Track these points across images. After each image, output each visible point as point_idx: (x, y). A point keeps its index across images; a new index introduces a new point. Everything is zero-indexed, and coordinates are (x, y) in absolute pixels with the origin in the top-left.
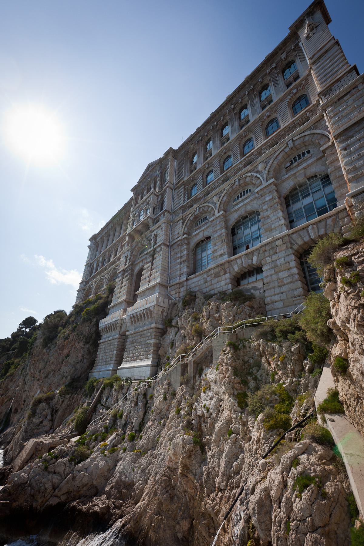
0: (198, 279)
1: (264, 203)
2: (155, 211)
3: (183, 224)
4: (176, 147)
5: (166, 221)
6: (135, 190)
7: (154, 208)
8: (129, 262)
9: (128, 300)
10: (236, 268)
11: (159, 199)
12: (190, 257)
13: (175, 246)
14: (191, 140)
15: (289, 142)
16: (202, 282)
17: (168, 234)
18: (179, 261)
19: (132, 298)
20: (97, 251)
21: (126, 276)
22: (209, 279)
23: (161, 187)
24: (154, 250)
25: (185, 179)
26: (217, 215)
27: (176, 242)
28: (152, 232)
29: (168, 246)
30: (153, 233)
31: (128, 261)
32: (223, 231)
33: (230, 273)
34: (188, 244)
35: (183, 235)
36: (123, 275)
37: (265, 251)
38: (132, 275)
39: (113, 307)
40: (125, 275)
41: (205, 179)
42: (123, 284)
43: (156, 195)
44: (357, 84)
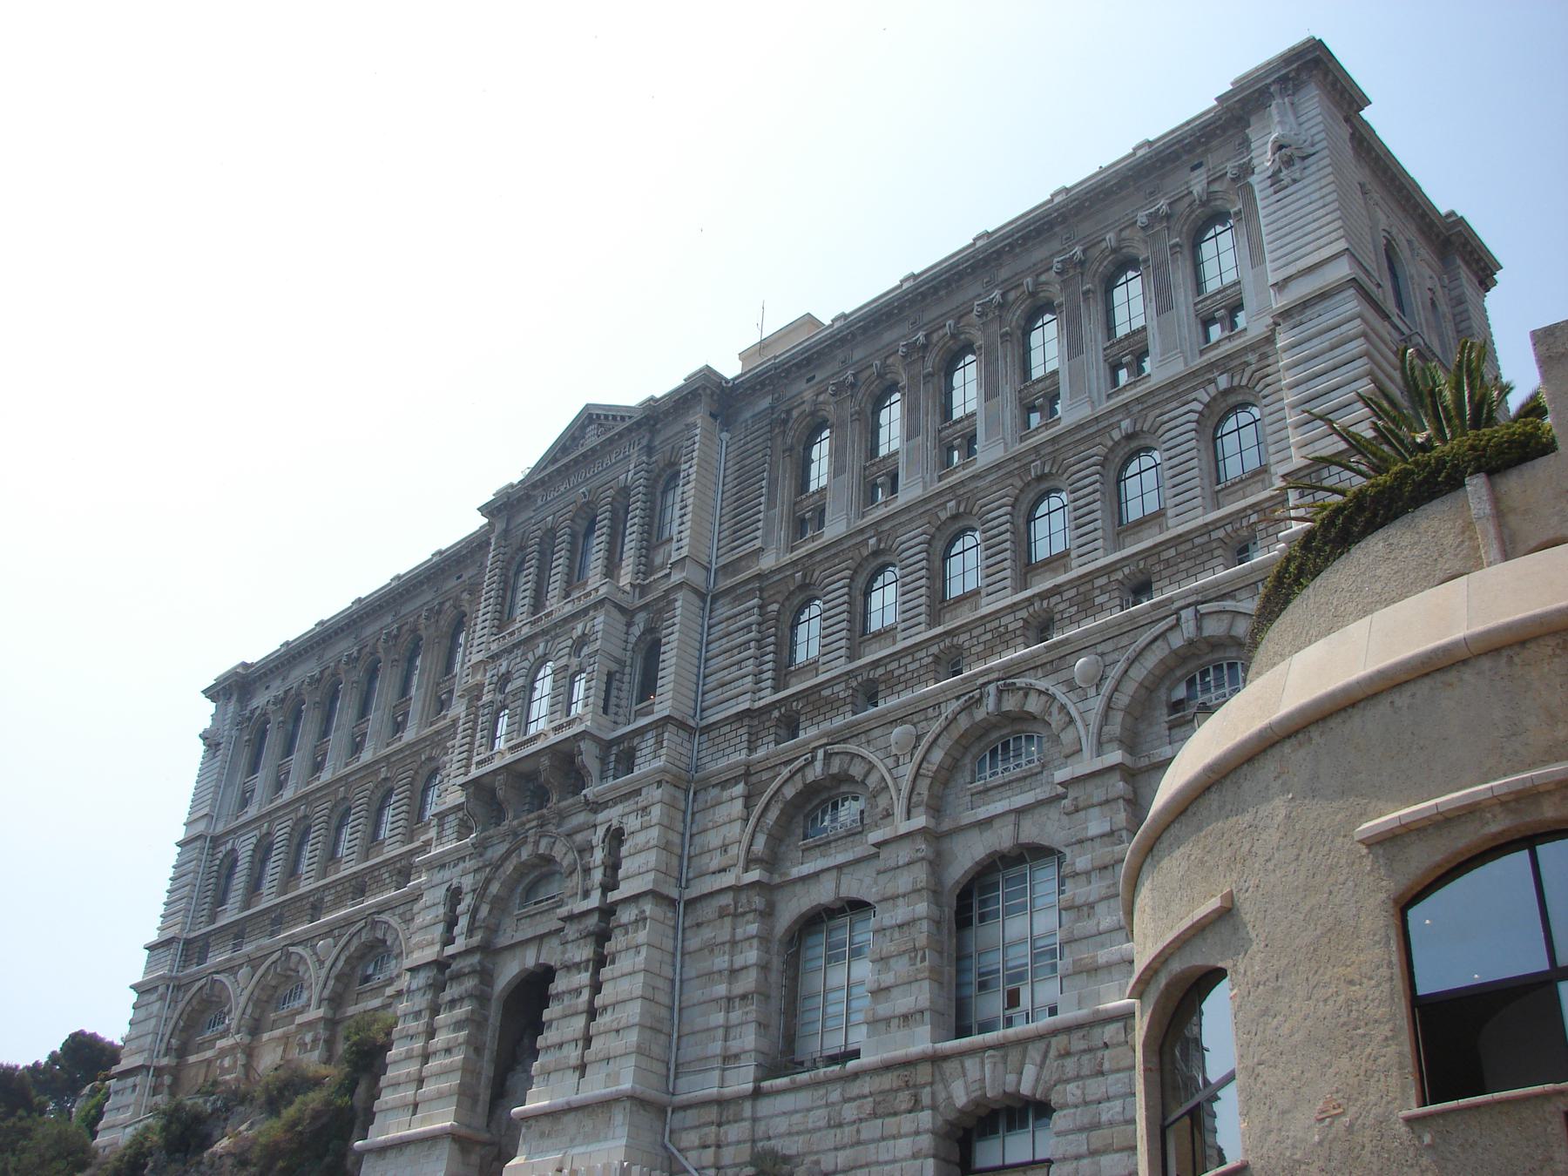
0: (803, 1099)
1: (1080, 842)
2: (614, 692)
3: (748, 806)
5: (668, 777)
6: (503, 507)
7: (610, 675)
8: (470, 932)
9: (464, 1131)
10: (961, 1097)
11: (637, 631)
12: (774, 977)
13: (709, 910)
14: (809, 360)
15: (1183, 613)
16: (818, 1117)
17: (676, 839)
18: (721, 989)
19: (480, 1119)
20: (254, 768)
21: (453, 1003)
22: (850, 1112)
23: (646, 566)
24: (607, 911)
25: (767, 562)
26: (904, 827)
27: (711, 894)
28: (595, 807)
29: (672, 903)
30: (601, 817)
31: (463, 922)
32: (922, 908)
33: (934, 1108)
34: (768, 913)
35: (746, 870)
37: (1068, 1054)
38: (481, 998)
39: (383, 1150)
40: (447, 995)
42: (441, 1039)
43: (622, 610)
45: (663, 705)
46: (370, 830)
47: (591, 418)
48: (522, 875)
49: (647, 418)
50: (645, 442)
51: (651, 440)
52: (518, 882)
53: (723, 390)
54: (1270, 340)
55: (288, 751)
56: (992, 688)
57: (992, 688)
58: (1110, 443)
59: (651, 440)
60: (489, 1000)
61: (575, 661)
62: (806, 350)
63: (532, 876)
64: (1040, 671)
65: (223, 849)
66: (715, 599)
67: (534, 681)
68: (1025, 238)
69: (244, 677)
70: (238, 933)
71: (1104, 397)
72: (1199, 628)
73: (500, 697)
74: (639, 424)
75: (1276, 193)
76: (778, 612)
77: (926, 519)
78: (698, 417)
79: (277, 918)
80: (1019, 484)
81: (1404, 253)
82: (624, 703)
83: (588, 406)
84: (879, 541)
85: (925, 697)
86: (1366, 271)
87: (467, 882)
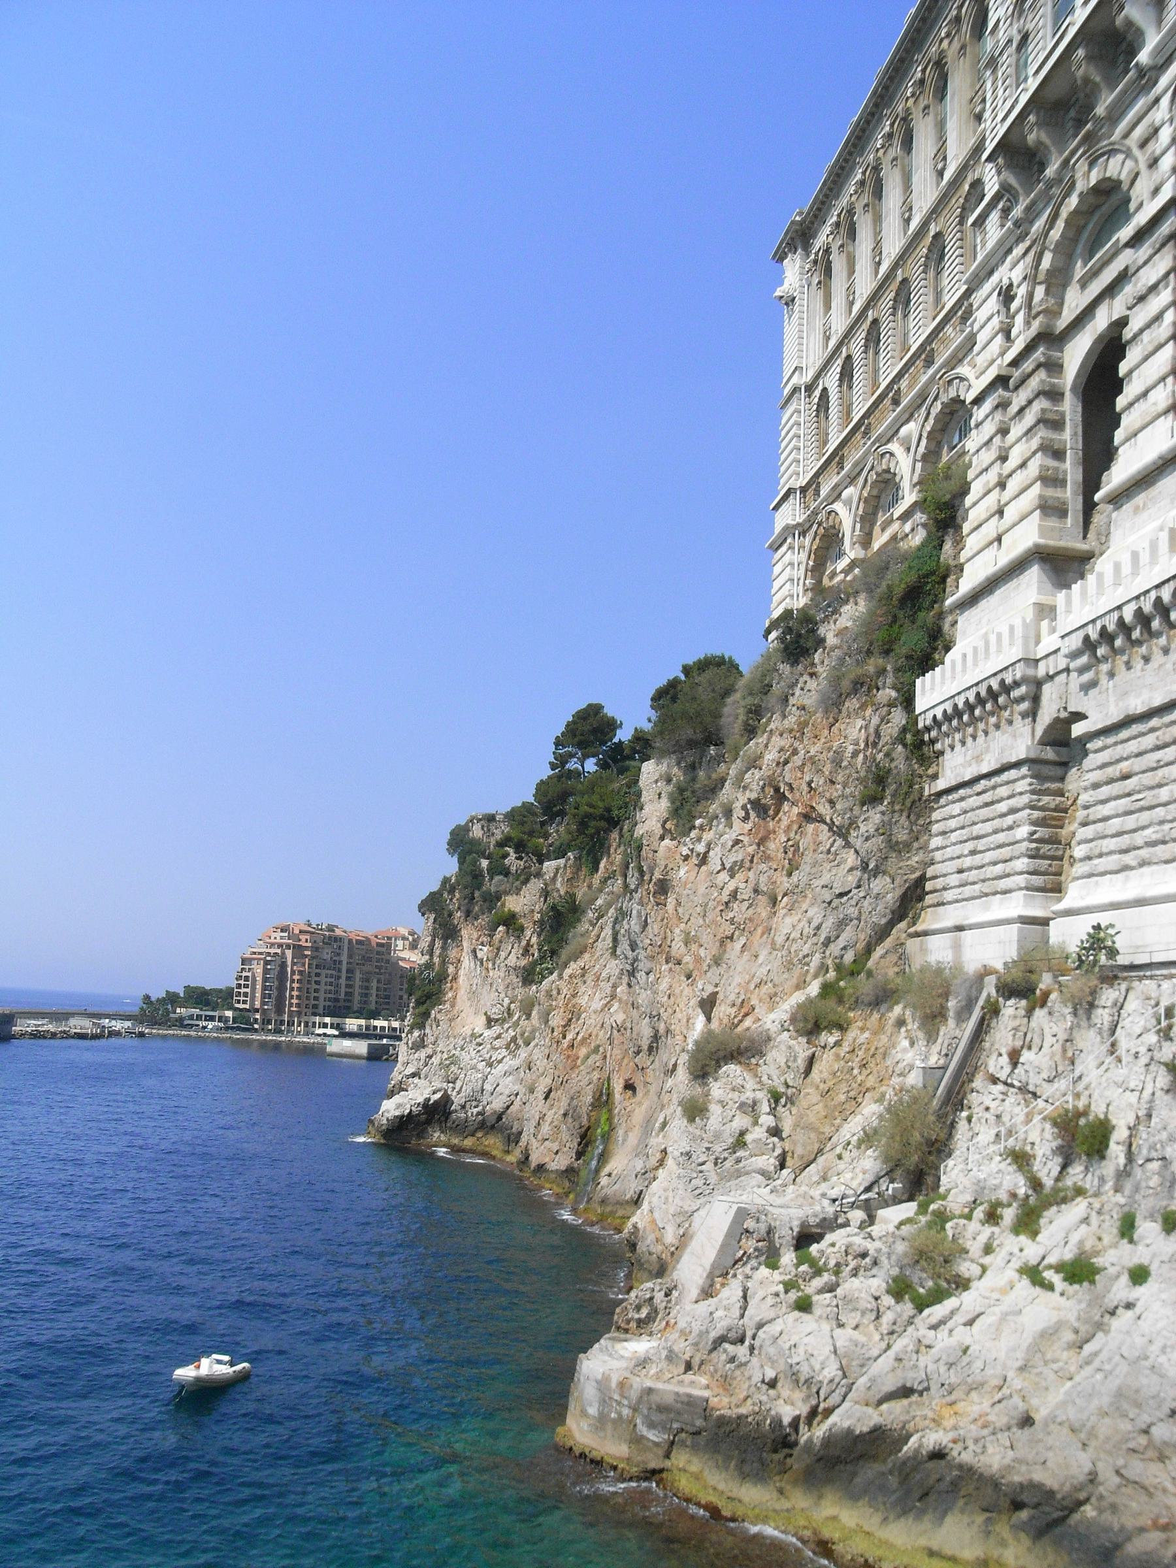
8: (1028, 323)
20: (828, 306)
36: (1003, 405)
39: (973, 599)
40: (1014, 409)
48: (1080, 230)
52: (1075, 241)
55: (851, 271)
60: (1062, 394)
63: (1090, 226)
65: (817, 393)
69: (801, 223)
70: (837, 458)
79: (862, 427)
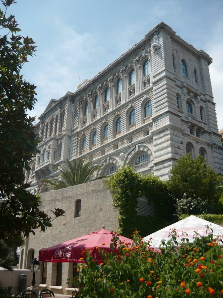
4: (74, 90)
7: (55, 152)
14: (84, 90)
25: (78, 130)
41: (92, 138)
43: (56, 139)
44: (167, 127)
45: (62, 159)
46: (28, 176)
47: (53, 101)
49: (60, 102)
50: (60, 106)
51: (61, 106)
53: (71, 96)
54: (152, 88)
56: (108, 158)
57: (108, 158)
58: (128, 109)
59: (61, 106)
61: (49, 149)
62: (84, 88)
64: (115, 155)
66: (71, 137)
67: (44, 153)
68: (116, 65)
71: (128, 99)
72: (139, 149)
73: (40, 155)
74: (59, 103)
75: (155, 56)
76: (80, 140)
77: (101, 123)
78: (68, 102)
80: (114, 116)
81: (187, 61)
82: (57, 157)
83: (52, 99)
84: (94, 127)
85: (98, 159)
86: (171, 73)
87: (37, 189)
